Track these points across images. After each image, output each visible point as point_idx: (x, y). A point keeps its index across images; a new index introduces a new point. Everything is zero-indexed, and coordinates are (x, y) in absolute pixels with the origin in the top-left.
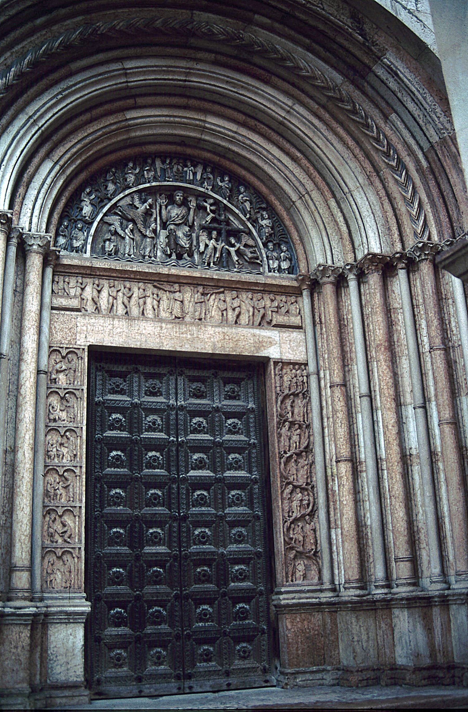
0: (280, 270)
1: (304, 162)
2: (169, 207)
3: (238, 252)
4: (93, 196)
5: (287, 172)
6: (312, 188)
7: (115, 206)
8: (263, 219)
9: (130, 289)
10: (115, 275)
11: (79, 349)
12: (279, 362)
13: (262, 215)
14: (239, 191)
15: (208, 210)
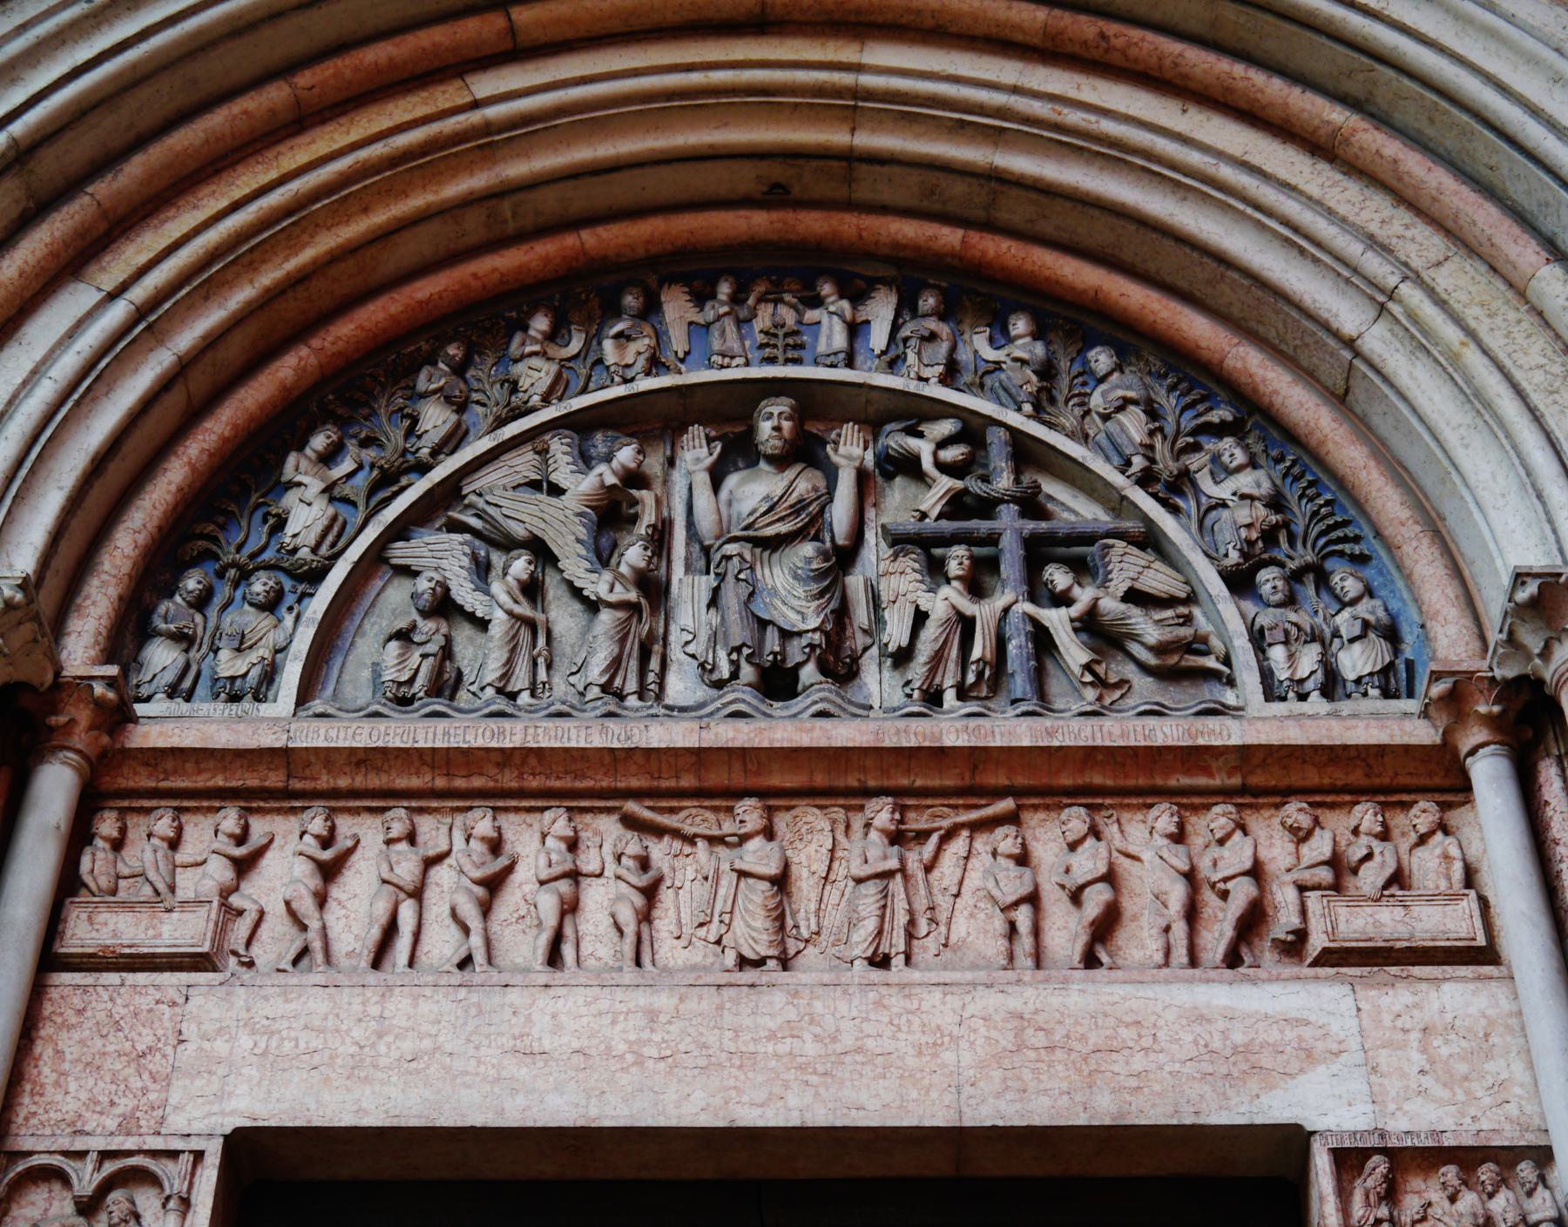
0: (1332, 685)
1: (1371, 140)
2: (732, 481)
3: (1090, 625)
4: (347, 466)
5: (1291, 207)
6: (1434, 255)
7: (450, 491)
8: (1221, 470)
9: (495, 846)
10: (415, 782)
11: (173, 1155)
12: (1366, 1153)
13: (1216, 458)
14: (1087, 371)
15: (927, 464)
